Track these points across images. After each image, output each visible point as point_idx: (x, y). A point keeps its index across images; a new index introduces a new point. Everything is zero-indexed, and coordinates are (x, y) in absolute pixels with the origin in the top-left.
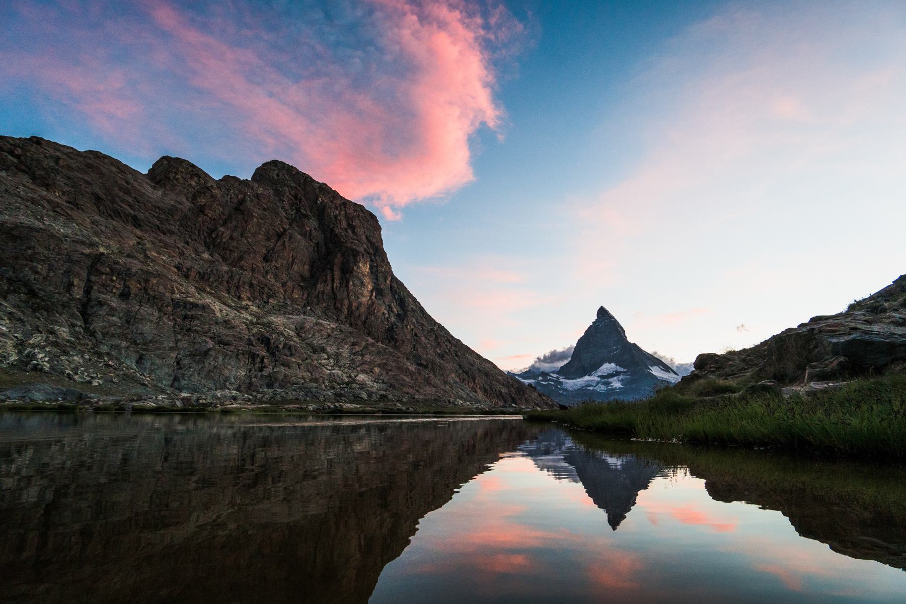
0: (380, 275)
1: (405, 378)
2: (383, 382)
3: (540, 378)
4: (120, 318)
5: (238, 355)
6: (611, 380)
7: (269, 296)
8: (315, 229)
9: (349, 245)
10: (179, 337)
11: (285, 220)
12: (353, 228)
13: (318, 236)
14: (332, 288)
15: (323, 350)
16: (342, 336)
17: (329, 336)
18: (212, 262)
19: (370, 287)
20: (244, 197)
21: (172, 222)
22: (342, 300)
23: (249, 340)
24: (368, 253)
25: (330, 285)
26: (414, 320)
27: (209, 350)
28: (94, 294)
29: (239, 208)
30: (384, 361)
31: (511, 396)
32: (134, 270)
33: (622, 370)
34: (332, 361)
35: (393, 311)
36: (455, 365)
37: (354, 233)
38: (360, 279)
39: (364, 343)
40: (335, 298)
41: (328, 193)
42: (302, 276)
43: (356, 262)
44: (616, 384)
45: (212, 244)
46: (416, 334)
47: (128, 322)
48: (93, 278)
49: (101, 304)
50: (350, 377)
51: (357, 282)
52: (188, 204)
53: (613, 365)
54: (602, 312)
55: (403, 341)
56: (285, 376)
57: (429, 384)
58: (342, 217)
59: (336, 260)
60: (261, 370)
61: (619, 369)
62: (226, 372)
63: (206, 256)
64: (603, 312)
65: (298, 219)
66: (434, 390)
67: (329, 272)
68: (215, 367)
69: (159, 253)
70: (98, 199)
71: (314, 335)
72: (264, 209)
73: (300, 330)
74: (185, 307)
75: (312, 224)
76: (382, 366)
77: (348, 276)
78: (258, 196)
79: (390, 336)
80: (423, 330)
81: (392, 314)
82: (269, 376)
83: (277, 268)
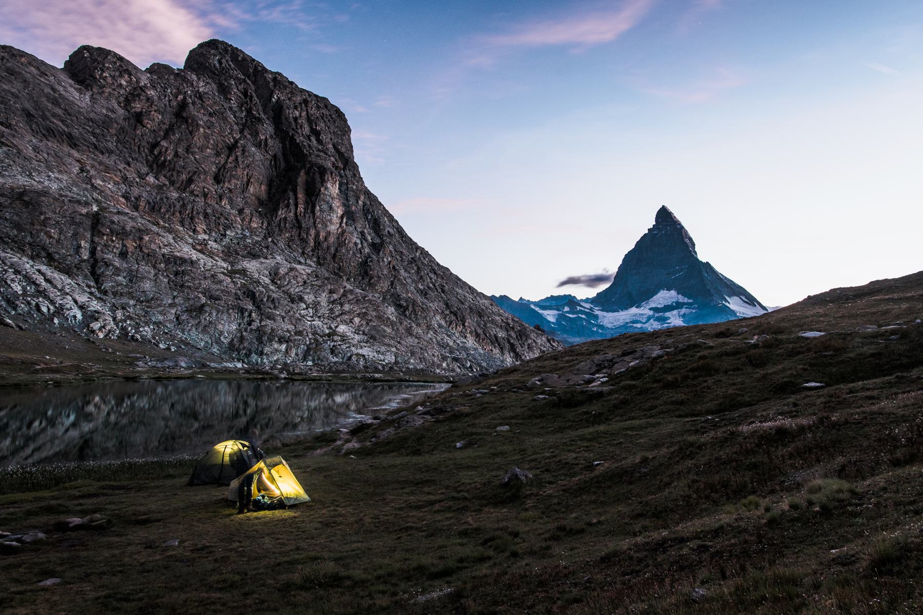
0: (351, 194)
1: (386, 329)
2: (364, 333)
3: (567, 309)
4: (125, 277)
5: (228, 310)
6: (667, 314)
7: (227, 227)
8: (271, 137)
9: (313, 158)
10: (175, 293)
11: (235, 127)
12: (317, 134)
13: (275, 146)
14: (296, 214)
15: (301, 299)
16: (319, 283)
17: (305, 282)
18: (160, 188)
19: (340, 212)
20: (185, 98)
21: (108, 138)
23: (236, 294)
24: (337, 168)
25: (293, 211)
26: (391, 247)
27: (203, 305)
28: (99, 255)
29: (181, 113)
30: (364, 311)
32: (128, 228)
33: (686, 300)
34: (310, 310)
35: (366, 240)
36: (441, 304)
37: (319, 141)
38: (328, 203)
39: (342, 291)
40: (300, 227)
41: (285, 87)
42: (258, 199)
43: (323, 182)
44: (675, 320)
45: (158, 165)
46: (394, 267)
47: (131, 281)
48: (96, 239)
49: (107, 265)
50: (330, 328)
51: (325, 207)
52: (121, 111)
53: (673, 293)
54: (664, 216)
55: (379, 277)
56: (272, 330)
57: (411, 335)
58: (303, 121)
60: (249, 324)
61: (681, 299)
62: (220, 327)
63: (151, 179)
64: (664, 216)
65: (250, 124)
66: (416, 341)
67: (291, 194)
68: (210, 322)
69: (104, 181)
70: (29, 115)
71: (289, 282)
72: (210, 115)
73: (274, 275)
74: (175, 263)
75: (267, 130)
76: (362, 316)
78: (200, 96)
80: (402, 260)
81: (365, 244)
82: (258, 330)
83: (230, 191)
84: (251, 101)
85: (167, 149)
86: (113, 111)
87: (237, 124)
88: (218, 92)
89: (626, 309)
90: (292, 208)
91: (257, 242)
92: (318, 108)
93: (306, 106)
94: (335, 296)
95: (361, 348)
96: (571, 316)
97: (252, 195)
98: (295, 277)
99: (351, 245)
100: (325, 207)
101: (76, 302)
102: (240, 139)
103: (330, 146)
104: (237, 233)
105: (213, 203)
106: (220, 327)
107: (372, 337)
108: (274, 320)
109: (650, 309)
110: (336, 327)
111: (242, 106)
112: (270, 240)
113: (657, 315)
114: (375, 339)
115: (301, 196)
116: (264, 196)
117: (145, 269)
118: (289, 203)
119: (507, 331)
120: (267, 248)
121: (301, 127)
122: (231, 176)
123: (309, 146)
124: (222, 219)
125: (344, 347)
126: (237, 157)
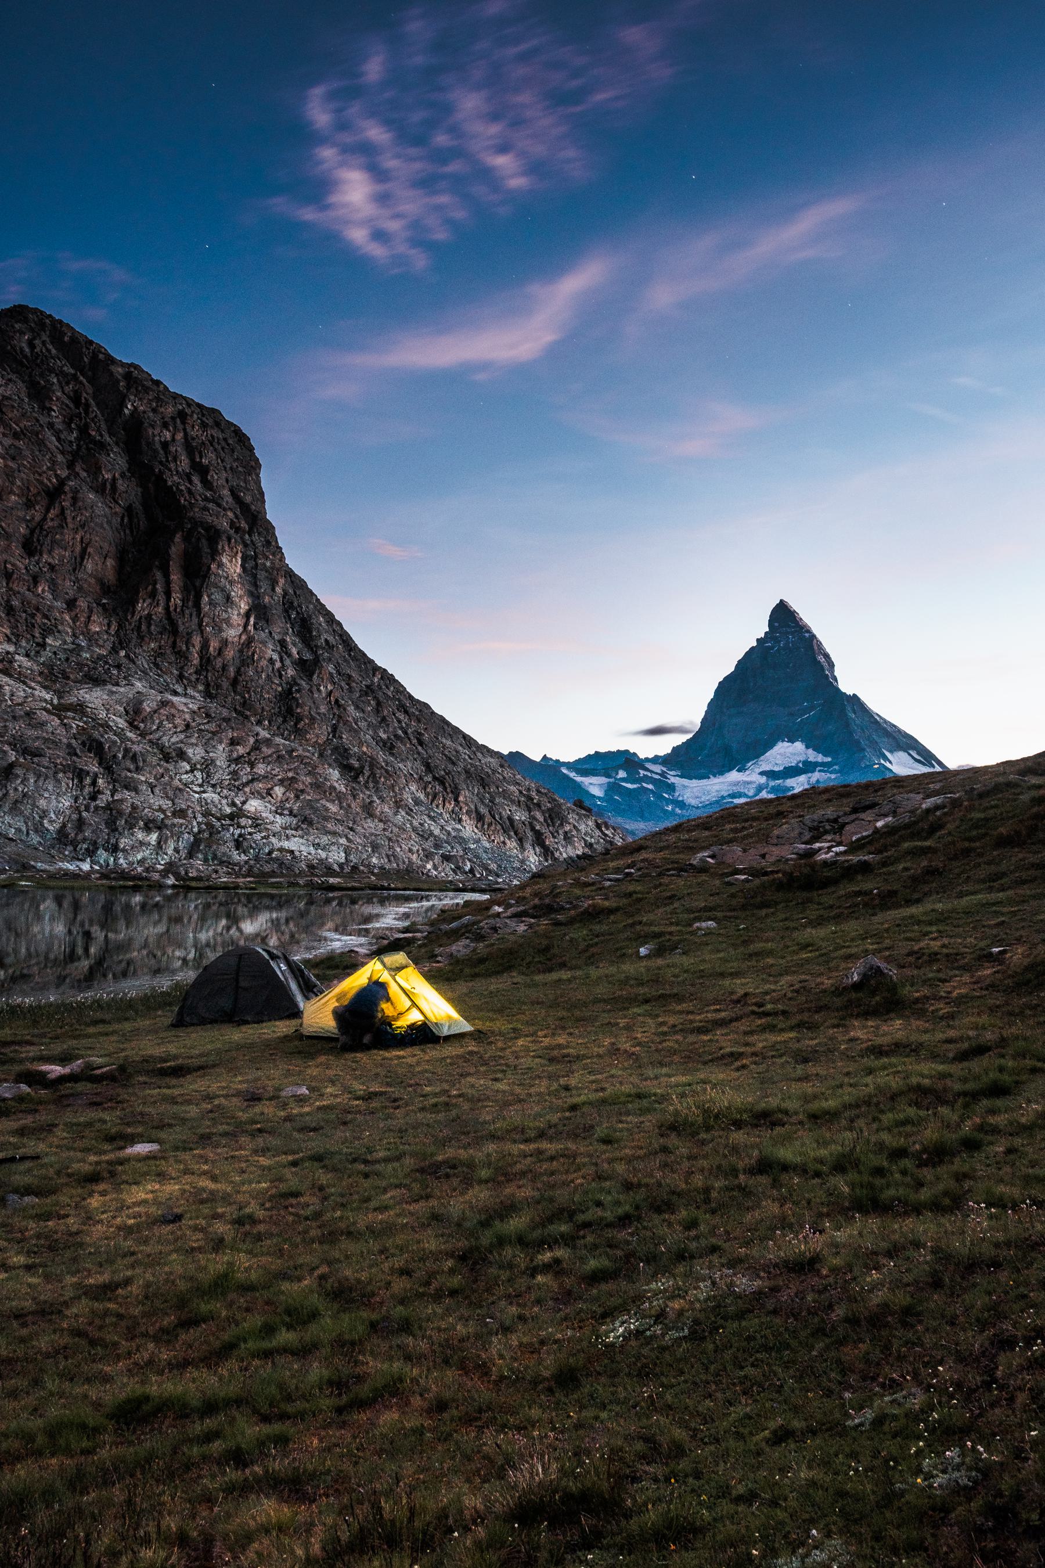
0: (262, 575)
1: (328, 805)
2: (291, 813)
3: (622, 774)
5: (56, 773)
7: (46, 631)
9: (196, 513)
11: (60, 458)
12: (202, 471)
13: (129, 490)
15: (182, 755)
16: (212, 727)
17: (188, 726)
19: (244, 606)
22: (189, 635)
23: (69, 745)
24: (238, 530)
25: (162, 603)
26: (331, 668)
27: (12, 766)
30: (290, 774)
31: (533, 829)
33: (820, 758)
34: (198, 774)
35: (289, 655)
36: (418, 764)
37: (207, 484)
38: (223, 590)
39: (252, 740)
40: (175, 632)
41: (147, 390)
42: (101, 581)
43: (215, 553)
46: (337, 701)
50: (234, 804)
51: (217, 597)
53: (799, 746)
55: (313, 719)
56: (134, 807)
59: (173, 550)
60: (93, 797)
61: (813, 756)
62: (42, 803)
65: (85, 453)
66: (381, 825)
67: (159, 575)
68: (25, 795)
72: (16, 436)
73: (134, 713)
76: (288, 783)
80: (351, 690)
81: (288, 662)
82: (108, 807)
83: (52, 568)
84: (87, 413)
87: (62, 453)
88: (29, 396)
89: (722, 773)
90: (161, 597)
91: (100, 657)
92: (204, 426)
93: (183, 423)
94: (241, 750)
95: (288, 838)
96: (629, 786)
97: (90, 575)
98: (171, 718)
99: (264, 663)
100: (217, 597)
102: (68, 478)
103: (226, 492)
104: (65, 642)
105: (23, 590)
106: (42, 803)
108: (136, 790)
109: (762, 773)
110: (244, 803)
111: (71, 421)
112: (123, 653)
113: (772, 783)
114: (311, 824)
115: (175, 577)
116: (110, 576)
118: (155, 590)
119: (530, 810)
120: (118, 667)
121: (175, 459)
122: (54, 542)
123: (190, 492)
124: (39, 618)
125: (258, 837)
126: (63, 509)
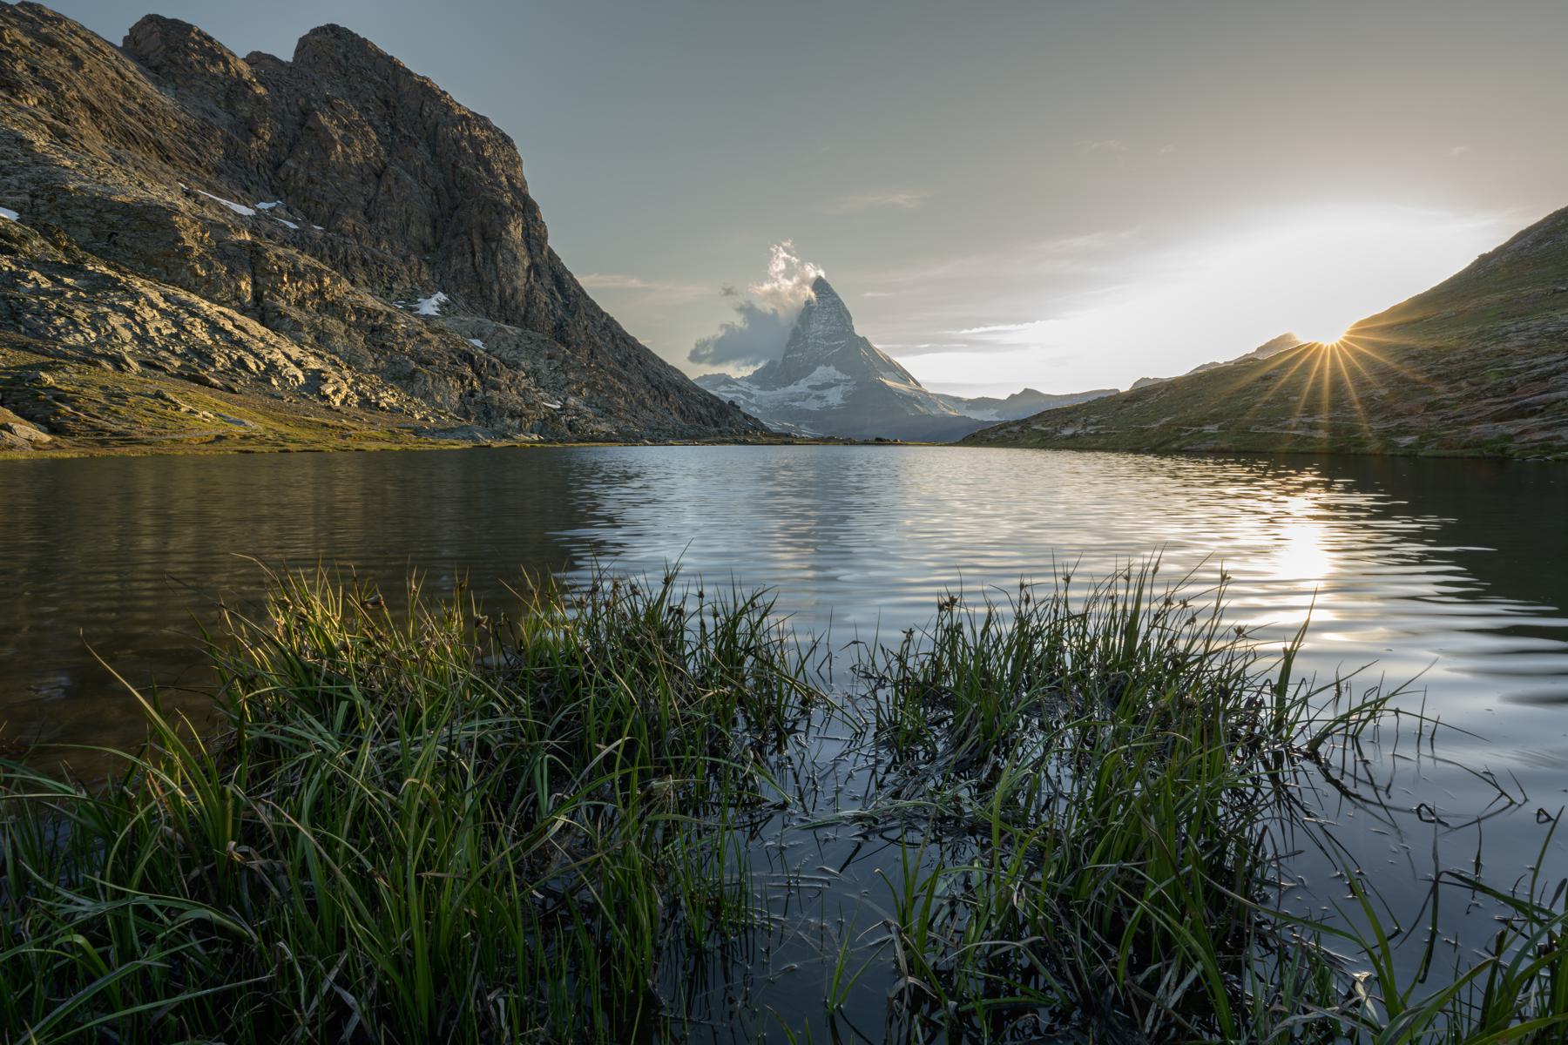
0: (533, 242)
6: (825, 393)
7: (392, 279)
15: (517, 366)
19: (526, 263)
22: (491, 284)
33: (844, 377)
43: (504, 225)
51: (508, 256)
52: (223, 115)
53: (832, 369)
61: (839, 376)
70: (93, 109)
75: (420, 155)
76: (591, 386)
77: (494, 245)
79: (560, 333)
85: (296, 172)
86: (213, 115)
90: (468, 256)
94: (556, 363)
100: (508, 256)
101: (288, 357)
107: (608, 411)
116: (430, 241)
117: (332, 323)
